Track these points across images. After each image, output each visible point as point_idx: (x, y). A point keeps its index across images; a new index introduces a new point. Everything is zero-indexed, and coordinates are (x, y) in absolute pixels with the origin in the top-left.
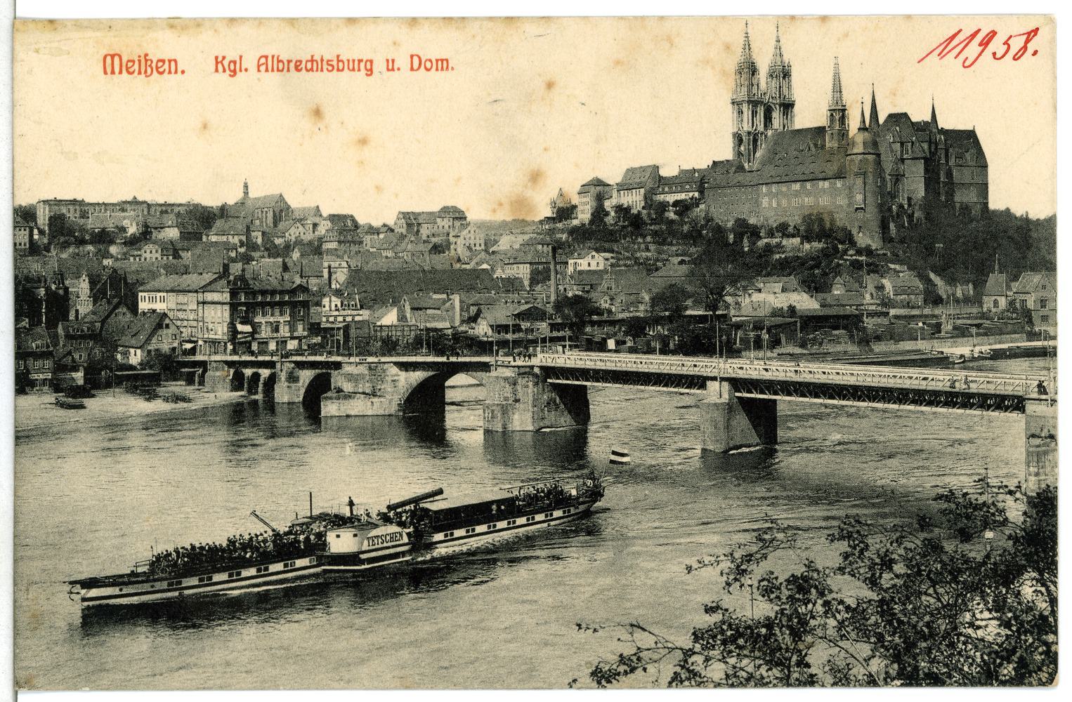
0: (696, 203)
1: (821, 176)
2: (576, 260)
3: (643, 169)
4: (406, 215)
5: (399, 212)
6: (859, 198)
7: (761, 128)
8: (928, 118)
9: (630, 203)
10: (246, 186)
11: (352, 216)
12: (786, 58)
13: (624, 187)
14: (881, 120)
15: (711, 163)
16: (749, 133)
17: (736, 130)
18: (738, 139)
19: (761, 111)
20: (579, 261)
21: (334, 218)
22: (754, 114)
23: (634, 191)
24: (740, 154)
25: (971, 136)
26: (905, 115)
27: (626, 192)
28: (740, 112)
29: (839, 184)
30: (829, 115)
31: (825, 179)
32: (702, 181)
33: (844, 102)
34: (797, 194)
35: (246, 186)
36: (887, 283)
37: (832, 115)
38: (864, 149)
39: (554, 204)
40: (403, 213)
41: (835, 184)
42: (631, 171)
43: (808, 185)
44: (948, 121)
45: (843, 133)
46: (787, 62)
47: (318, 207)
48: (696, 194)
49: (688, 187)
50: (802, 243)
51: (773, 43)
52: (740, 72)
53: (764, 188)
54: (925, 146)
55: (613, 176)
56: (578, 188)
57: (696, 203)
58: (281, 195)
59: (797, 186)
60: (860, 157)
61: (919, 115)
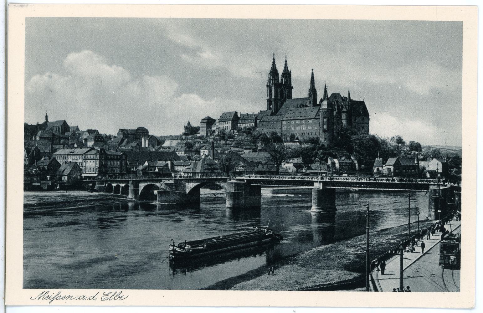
0: (254, 128)
1: (309, 117)
2: (204, 150)
3: (230, 113)
4: (122, 131)
5: (120, 129)
6: (325, 127)
8: (347, 96)
9: (225, 127)
10: (47, 117)
11: (97, 131)
13: (222, 120)
14: (329, 96)
15: (259, 112)
16: (275, 100)
17: (268, 98)
18: (269, 102)
20: (205, 151)
21: (90, 131)
23: (226, 122)
24: (270, 109)
25: (362, 103)
26: (339, 94)
27: (223, 123)
28: (271, 91)
29: (316, 121)
30: (309, 93)
32: (257, 119)
33: (315, 88)
34: (298, 125)
35: (47, 117)
36: (336, 161)
37: (310, 93)
38: (328, 108)
39: (186, 128)
40: (121, 130)
41: (315, 121)
42: (225, 114)
44: (354, 98)
45: (315, 100)
47: (77, 126)
48: (254, 124)
49: (250, 121)
50: (301, 144)
51: (284, 63)
52: (270, 74)
54: (347, 107)
55: (216, 116)
56: (201, 121)
57: (254, 128)
58: (65, 123)
59: (298, 122)
60: (326, 110)
61: (344, 94)
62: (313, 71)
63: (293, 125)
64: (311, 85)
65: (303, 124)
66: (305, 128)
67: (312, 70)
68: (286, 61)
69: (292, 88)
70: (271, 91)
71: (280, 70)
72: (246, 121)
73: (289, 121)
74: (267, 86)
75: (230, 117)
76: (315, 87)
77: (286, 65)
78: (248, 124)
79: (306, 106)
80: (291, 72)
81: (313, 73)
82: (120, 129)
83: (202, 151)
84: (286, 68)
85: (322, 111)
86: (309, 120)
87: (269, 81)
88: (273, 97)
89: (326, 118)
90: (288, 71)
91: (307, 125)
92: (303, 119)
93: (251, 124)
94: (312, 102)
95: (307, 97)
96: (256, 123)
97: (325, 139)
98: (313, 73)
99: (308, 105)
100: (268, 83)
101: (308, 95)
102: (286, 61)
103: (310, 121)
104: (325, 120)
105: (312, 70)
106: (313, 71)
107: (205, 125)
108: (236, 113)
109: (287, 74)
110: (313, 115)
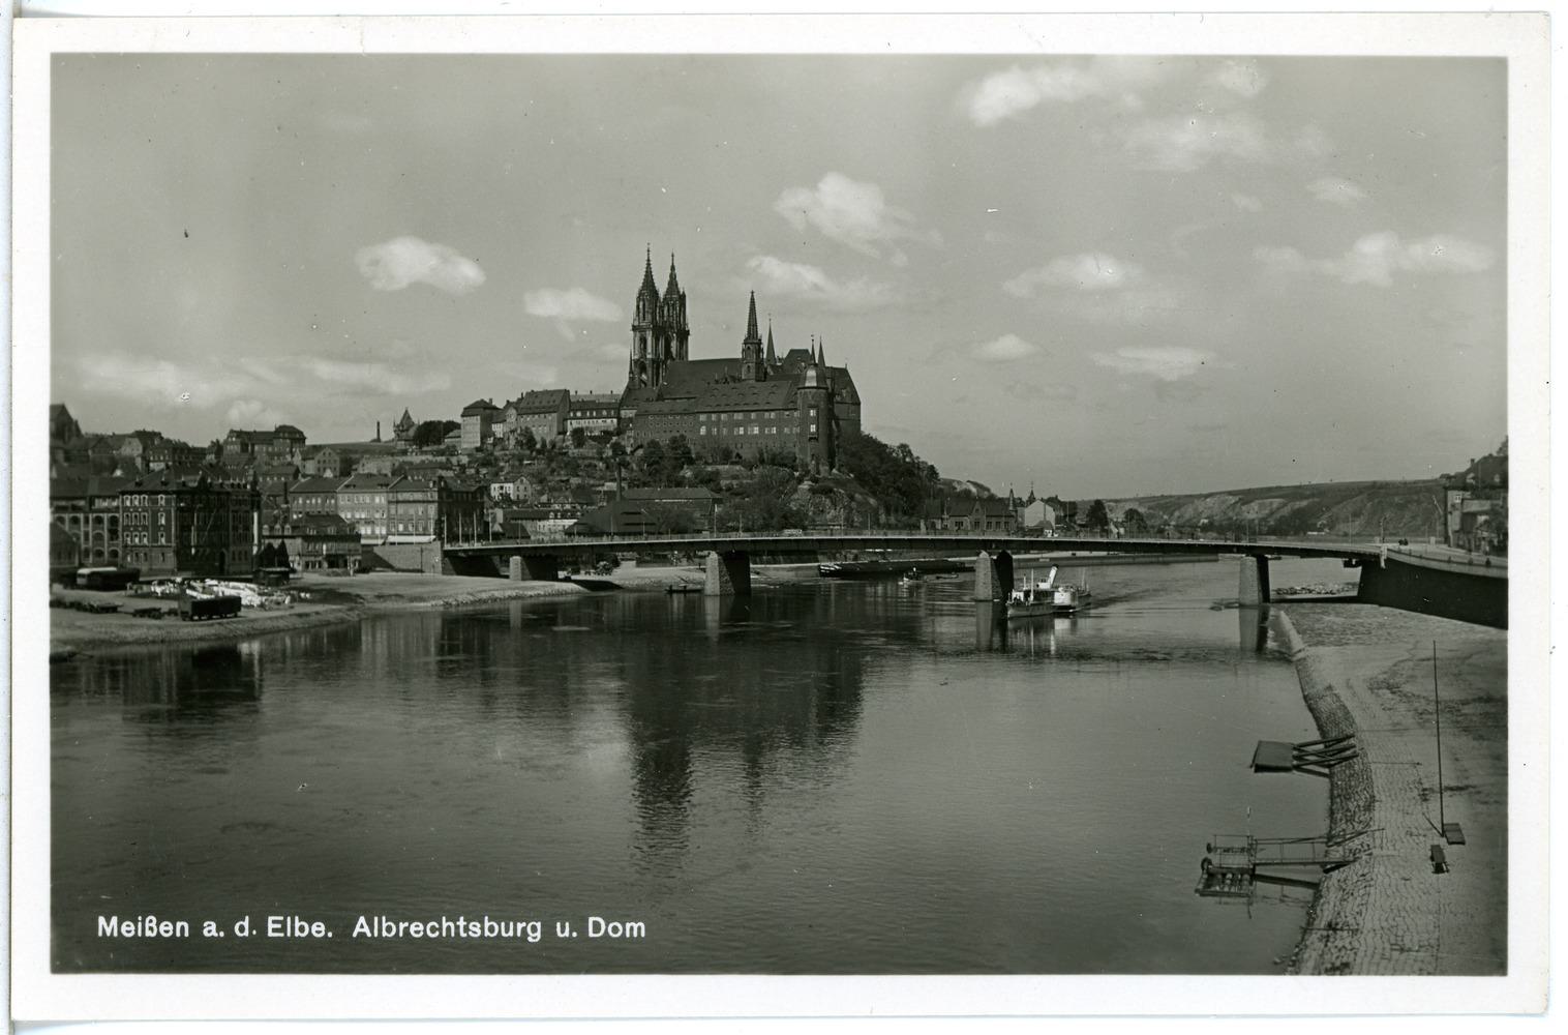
6: (813, 428)
7: (662, 357)
12: (682, 286)
16: (653, 361)
19: (662, 342)
22: (656, 339)
28: (643, 341)
31: (772, 410)
34: (738, 424)
43: (753, 415)
48: (615, 420)
49: (605, 413)
53: (703, 418)
56: (461, 411)
59: (739, 417)
60: (815, 390)
62: (752, 296)
63: (725, 423)
65: (752, 421)
66: (756, 431)
68: (673, 268)
69: (688, 333)
70: (643, 341)
71: (662, 287)
72: (594, 414)
73: (714, 417)
74: (634, 328)
75: (551, 403)
77: (673, 277)
78: (600, 421)
79: (740, 380)
80: (686, 293)
82: (232, 431)
83: (497, 485)
85: (805, 393)
86: (767, 414)
87: (638, 315)
88: (649, 356)
89: (812, 407)
90: (678, 292)
91: (763, 424)
92: (753, 411)
93: (609, 421)
94: (753, 370)
95: (739, 356)
96: (619, 419)
97: (813, 455)
99: (743, 377)
100: (634, 320)
102: (673, 268)
103: (773, 414)
104: (812, 413)
106: (752, 296)
107: (477, 420)
109: (677, 299)
110: (778, 400)
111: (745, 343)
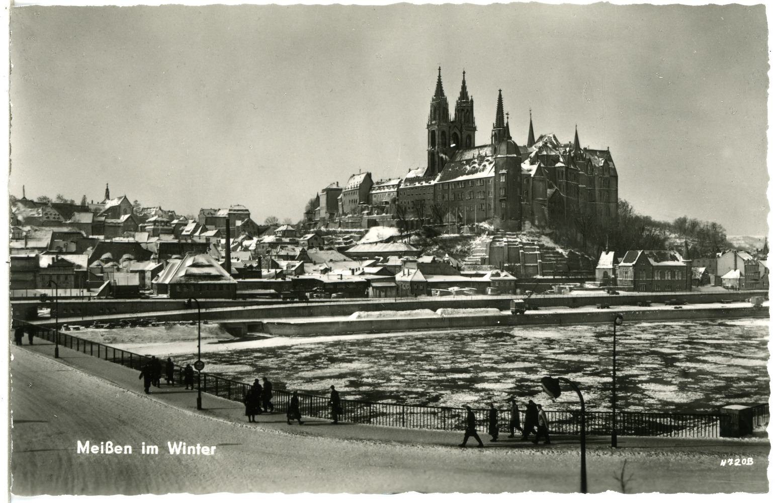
6: (502, 193)
12: (469, 94)
37: (495, 134)
46: (470, 98)
62: (500, 93)
64: (497, 119)
67: (500, 91)
69: (474, 129)
76: (505, 121)
77: (464, 87)
80: (474, 100)
81: (500, 96)
84: (463, 94)
98: (500, 96)
101: (492, 138)
105: (500, 91)
106: (500, 93)
108: (369, 175)
111: (493, 131)
